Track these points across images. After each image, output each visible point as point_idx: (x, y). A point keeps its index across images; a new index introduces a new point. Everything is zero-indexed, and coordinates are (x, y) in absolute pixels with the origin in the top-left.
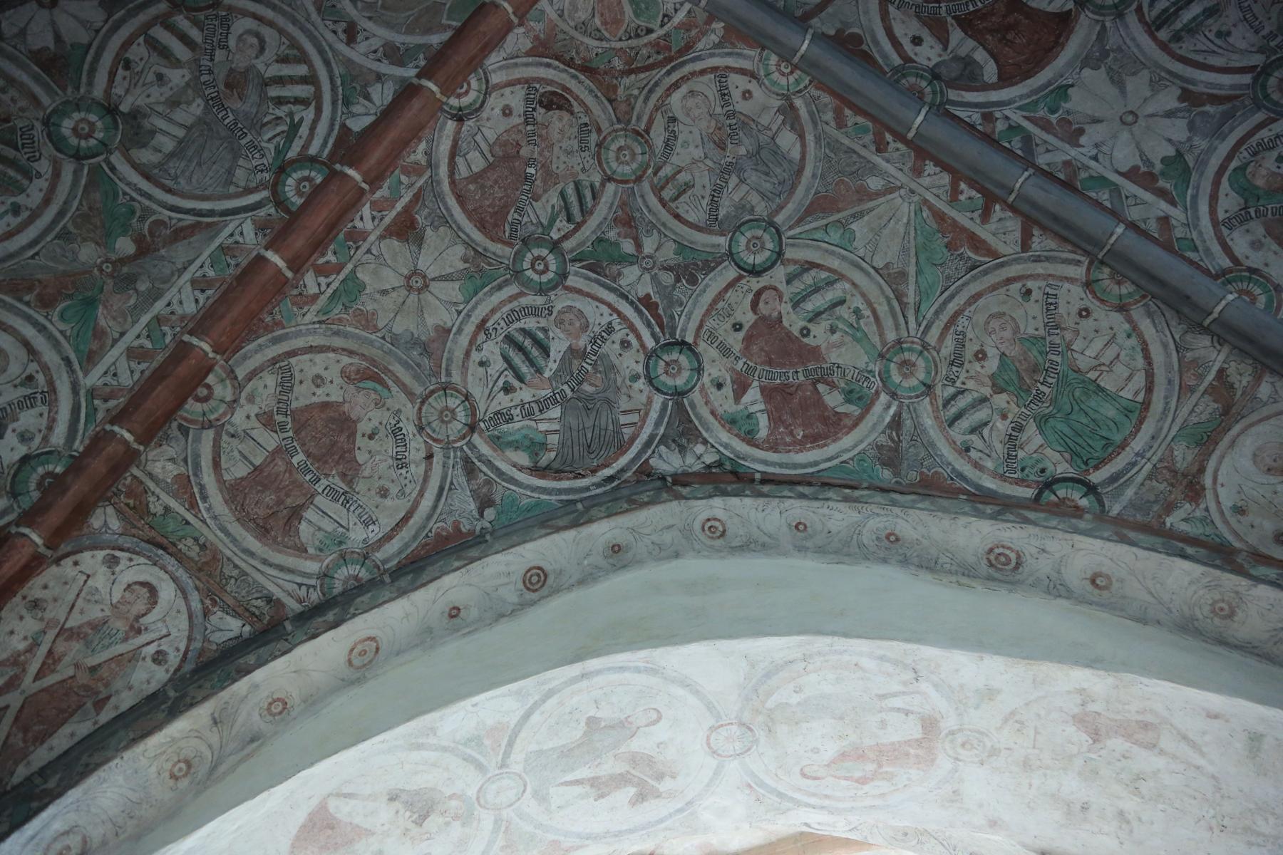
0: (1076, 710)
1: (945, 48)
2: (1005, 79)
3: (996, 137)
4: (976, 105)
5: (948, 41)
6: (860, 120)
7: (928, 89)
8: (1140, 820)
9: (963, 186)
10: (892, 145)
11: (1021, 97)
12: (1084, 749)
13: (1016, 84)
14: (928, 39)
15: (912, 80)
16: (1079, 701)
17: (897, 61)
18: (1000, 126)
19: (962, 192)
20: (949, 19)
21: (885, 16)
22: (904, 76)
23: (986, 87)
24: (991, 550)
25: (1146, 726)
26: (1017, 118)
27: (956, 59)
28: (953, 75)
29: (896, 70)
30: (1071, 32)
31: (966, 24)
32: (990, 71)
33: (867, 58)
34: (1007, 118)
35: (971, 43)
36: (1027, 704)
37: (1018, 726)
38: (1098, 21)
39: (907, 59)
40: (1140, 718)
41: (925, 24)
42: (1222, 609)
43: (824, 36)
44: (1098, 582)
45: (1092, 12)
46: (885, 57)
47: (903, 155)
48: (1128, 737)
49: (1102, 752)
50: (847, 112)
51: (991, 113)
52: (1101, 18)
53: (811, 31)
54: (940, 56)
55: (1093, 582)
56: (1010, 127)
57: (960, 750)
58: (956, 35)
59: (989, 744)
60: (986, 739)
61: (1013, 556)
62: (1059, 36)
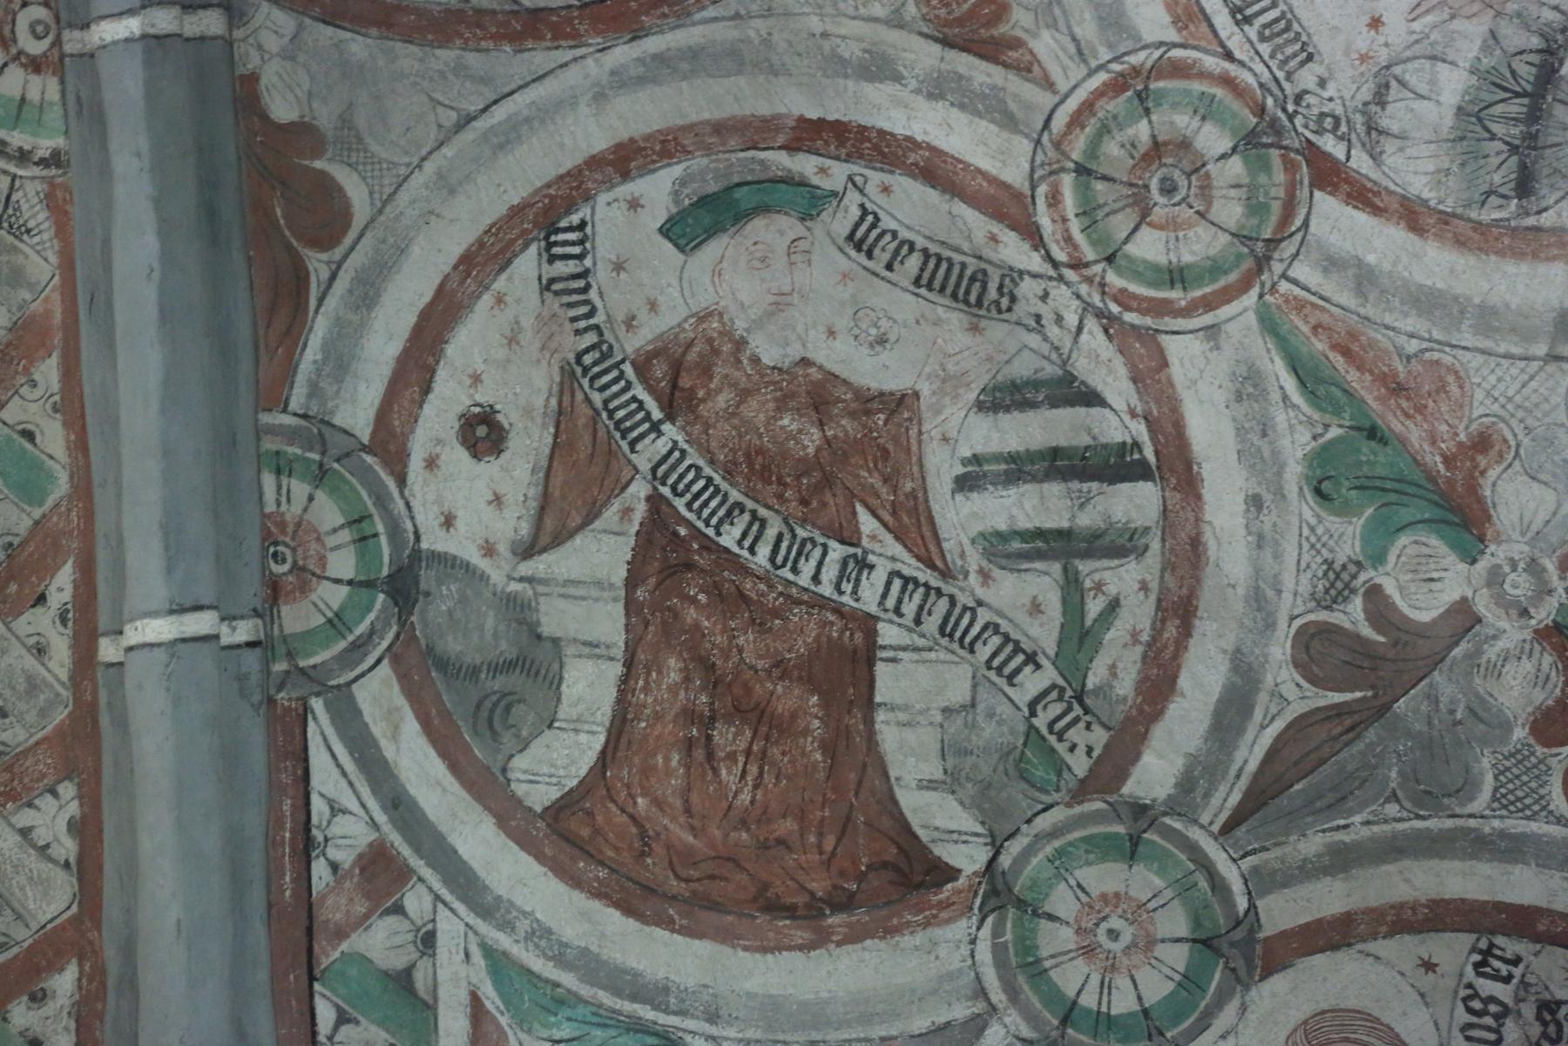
1: (528, 551)
2: (565, 833)
3: (329, 956)
4: (399, 804)
5: (558, 540)
6: (54, 438)
7: (335, 596)
9: (65, 983)
10: (41, 622)
11: (540, 934)
13: (576, 882)
14: (519, 468)
15: (328, 513)
17: (357, 412)
18: (381, 942)
19: (39, 998)
20: (639, 490)
21: (483, 260)
22: (320, 476)
23: (488, 788)
26: (454, 976)
27: (518, 611)
28: (452, 645)
29: (319, 429)
30: (889, 932)
31: (668, 558)
32: (553, 763)
33: (287, 300)
34: (428, 941)
35: (609, 623)
38: (981, 992)
39: (389, 443)
41: (562, 417)
43: (247, 95)
45: (999, 951)
46: (340, 363)
47: (33, 685)
50: (49, 372)
51: (404, 875)
52: (998, 996)
53: (210, 22)
54: (489, 550)
56: (403, 980)
58: (603, 552)
62: (844, 903)
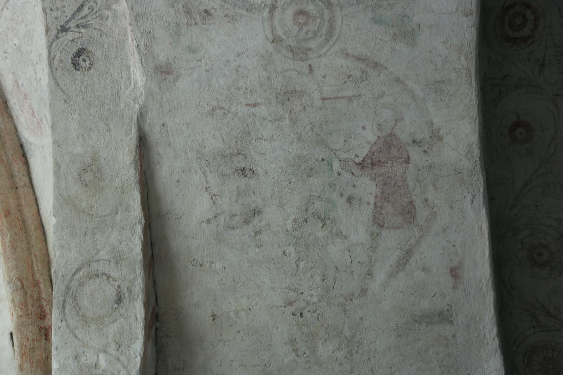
0: (404, 137)
8: (258, 232)
12: (344, 156)
16: (418, 137)
24: (528, 6)
25: (409, 213)
36: (397, 80)
37: (358, 74)
40: (418, 203)
42: (540, 254)
44: (519, 130)
48: (384, 197)
49: (346, 176)
55: (518, 124)
57: (290, 12)
59: (312, 44)
60: (319, 40)
61: (526, 32)
